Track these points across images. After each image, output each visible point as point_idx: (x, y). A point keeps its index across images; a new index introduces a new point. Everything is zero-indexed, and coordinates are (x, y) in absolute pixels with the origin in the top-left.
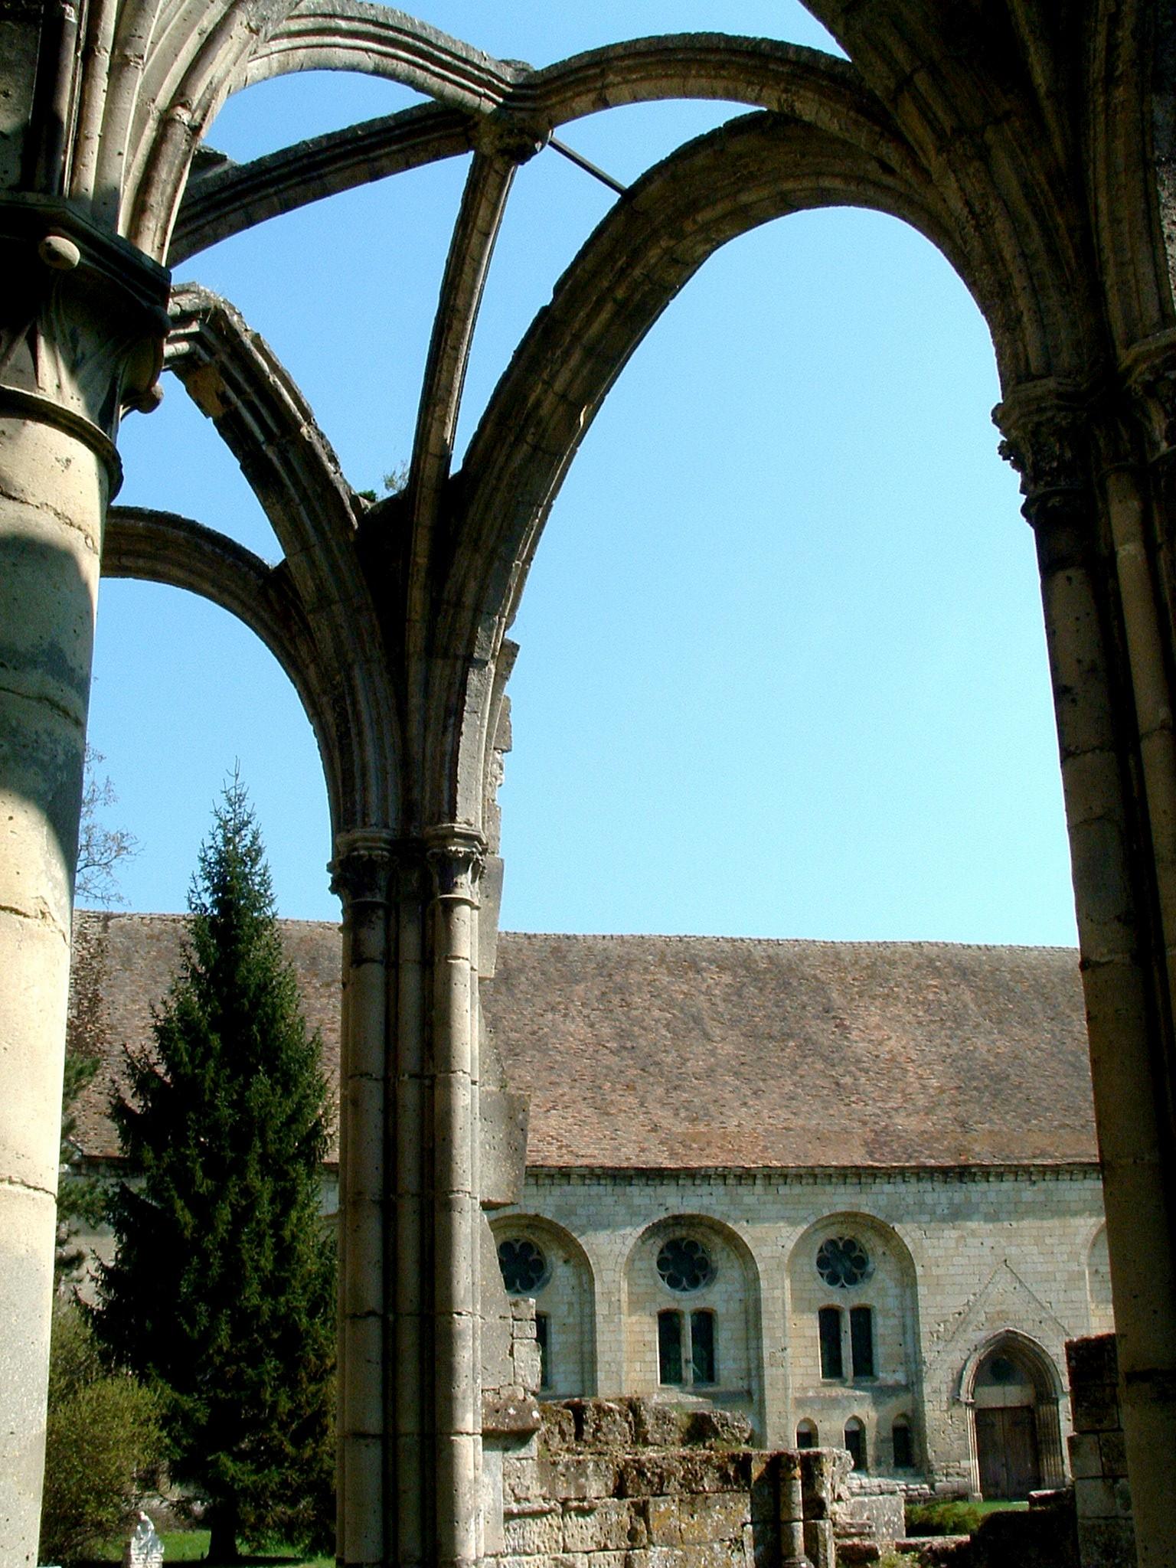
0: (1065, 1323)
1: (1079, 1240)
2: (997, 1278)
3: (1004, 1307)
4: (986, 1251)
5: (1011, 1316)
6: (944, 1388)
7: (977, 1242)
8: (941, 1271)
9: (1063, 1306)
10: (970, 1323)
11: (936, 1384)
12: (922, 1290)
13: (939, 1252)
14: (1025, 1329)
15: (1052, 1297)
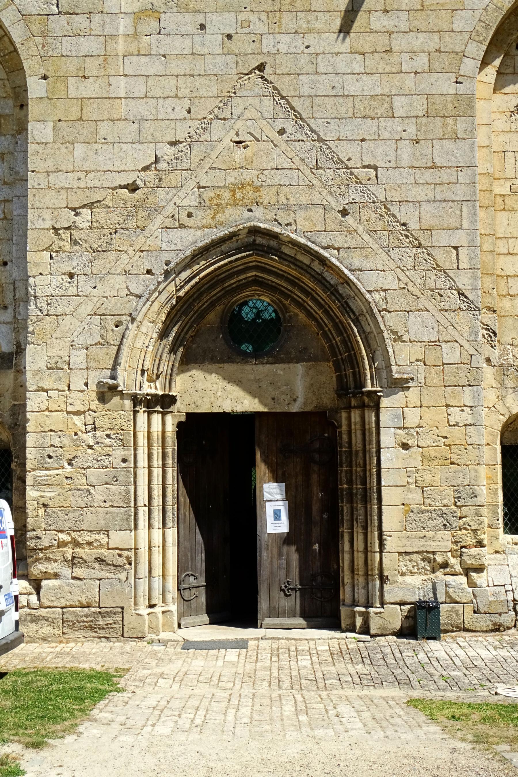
0: (410, 216)
1: (463, 22)
2: (237, 106)
3: (248, 176)
4: (213, 41)
5: (268, 196)
6: (79, 358)
7: (188, 22)
8: (89, 89)
9: (405, 176)
10: (158, 209)
11: (58, 349)
12: (39, 131)
13: (90, 45)
14: (304, 227)
15: (380, 153)
